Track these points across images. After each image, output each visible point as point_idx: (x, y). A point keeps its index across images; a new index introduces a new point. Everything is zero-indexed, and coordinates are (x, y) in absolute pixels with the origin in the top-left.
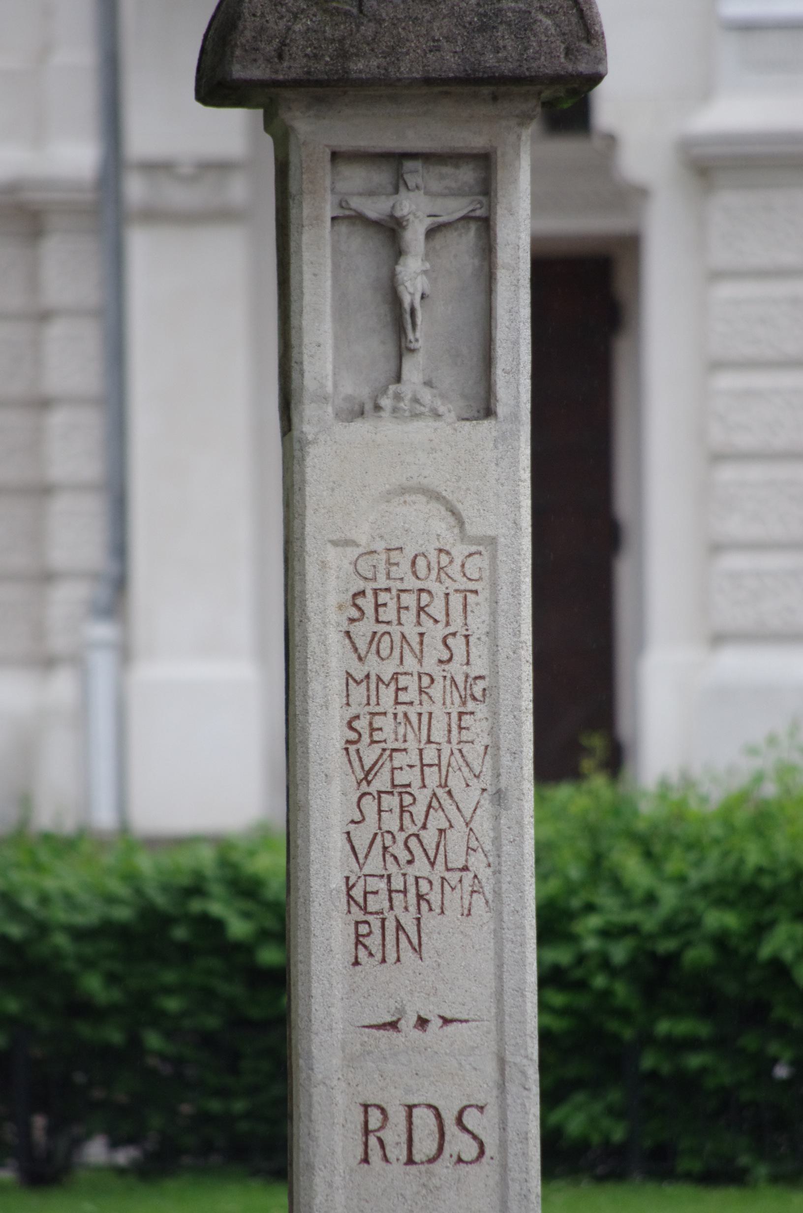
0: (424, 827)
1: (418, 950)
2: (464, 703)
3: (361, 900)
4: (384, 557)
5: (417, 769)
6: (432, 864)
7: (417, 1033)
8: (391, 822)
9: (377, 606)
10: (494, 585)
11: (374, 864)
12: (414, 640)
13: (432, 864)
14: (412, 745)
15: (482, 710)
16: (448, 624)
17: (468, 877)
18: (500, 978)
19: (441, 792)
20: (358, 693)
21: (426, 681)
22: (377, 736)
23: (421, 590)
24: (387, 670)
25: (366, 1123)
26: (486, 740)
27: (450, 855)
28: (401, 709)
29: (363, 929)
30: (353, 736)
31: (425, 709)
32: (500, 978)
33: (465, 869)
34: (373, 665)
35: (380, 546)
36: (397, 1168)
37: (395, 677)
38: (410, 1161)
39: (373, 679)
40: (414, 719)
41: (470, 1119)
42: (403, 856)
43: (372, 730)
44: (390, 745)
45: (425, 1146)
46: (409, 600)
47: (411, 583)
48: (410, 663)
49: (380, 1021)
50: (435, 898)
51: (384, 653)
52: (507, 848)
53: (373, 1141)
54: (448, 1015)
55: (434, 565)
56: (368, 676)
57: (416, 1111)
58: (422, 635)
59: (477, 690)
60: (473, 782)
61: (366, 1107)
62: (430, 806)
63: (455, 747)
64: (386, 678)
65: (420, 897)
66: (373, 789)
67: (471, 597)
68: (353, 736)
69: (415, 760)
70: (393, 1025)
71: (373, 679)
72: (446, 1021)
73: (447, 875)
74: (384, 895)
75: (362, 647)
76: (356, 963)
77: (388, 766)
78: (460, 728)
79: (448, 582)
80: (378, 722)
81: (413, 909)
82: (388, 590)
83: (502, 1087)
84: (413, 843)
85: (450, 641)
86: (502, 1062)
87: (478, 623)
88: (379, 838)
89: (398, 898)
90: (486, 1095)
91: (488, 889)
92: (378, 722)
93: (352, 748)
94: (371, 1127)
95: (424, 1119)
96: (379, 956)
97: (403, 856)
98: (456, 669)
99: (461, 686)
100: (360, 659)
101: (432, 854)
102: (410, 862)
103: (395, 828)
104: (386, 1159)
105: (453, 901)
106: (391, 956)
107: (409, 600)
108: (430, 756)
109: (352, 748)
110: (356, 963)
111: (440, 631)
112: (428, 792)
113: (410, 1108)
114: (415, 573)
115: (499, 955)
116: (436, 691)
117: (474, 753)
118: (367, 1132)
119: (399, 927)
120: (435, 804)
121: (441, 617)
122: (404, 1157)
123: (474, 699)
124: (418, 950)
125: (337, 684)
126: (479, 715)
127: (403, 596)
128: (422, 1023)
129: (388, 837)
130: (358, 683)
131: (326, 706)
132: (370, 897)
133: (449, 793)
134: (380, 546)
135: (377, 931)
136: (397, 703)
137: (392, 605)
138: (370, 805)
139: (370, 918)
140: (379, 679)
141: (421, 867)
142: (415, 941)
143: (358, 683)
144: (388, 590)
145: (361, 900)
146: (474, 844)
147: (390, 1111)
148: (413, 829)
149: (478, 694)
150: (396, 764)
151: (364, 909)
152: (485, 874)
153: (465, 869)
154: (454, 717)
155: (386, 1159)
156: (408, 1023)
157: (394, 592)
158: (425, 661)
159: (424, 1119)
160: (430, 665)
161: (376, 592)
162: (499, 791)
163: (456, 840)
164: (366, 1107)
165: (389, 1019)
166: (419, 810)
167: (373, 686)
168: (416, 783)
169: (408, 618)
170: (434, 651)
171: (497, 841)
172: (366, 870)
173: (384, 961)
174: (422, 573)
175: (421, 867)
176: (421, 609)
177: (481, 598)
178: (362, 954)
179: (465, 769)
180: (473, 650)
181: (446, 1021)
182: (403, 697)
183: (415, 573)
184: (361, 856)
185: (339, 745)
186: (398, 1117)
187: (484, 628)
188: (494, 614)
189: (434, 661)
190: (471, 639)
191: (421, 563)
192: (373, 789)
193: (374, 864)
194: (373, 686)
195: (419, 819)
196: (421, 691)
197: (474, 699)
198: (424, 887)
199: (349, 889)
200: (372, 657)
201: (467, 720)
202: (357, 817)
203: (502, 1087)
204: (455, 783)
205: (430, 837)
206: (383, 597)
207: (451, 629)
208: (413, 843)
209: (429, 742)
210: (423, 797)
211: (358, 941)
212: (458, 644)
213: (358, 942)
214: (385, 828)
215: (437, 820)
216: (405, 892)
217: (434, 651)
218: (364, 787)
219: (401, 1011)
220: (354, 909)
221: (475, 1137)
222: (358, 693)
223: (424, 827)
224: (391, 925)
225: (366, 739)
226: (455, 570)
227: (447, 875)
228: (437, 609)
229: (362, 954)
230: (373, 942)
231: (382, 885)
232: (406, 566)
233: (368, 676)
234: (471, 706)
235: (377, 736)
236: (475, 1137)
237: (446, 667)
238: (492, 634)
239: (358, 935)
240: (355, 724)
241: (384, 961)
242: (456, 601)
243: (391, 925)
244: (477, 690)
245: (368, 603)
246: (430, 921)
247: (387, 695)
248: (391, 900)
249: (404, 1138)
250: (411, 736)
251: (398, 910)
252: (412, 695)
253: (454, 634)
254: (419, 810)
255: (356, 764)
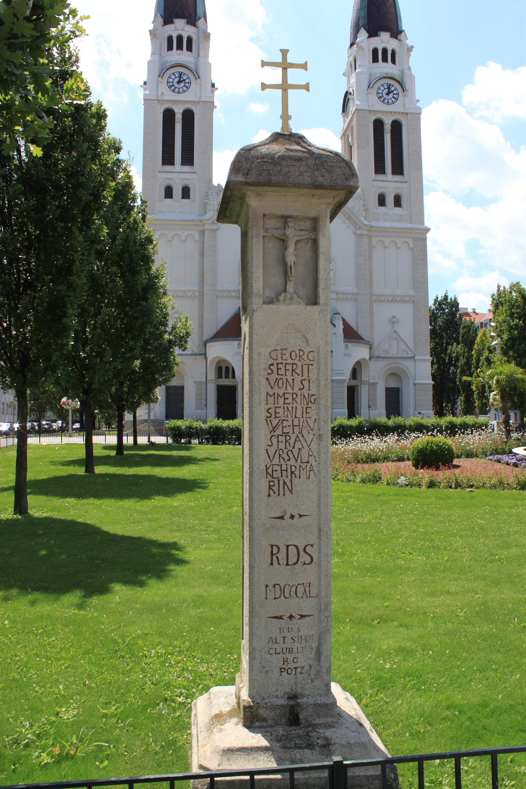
0: (294, 448)
1: (291, 491)
2: (308, 404)
3: (271, 473)
4: (280, 352)
5: (291, 427)
6: (296, 461)
7: (291, 520)
8: (282, 446)
9: (278, 369)
10: (319, 363)
11: (276, 461)
12: (291, 381)
13: (296, 461)
14: (290, 418)
15: (314, 407)
16: (302, 376)
17: (309, 465)
18: (319, 500)
19: (299, 435)
20: (271, 400)
21: (295, 396)
22: (277, 415)
23: (293, 364)
24: (281, 392)
25: (272, 551)
26: (315, 417)
27: (302, 457)
28: (286, 406)
29: (272, 484)
30: (269, 415)
31: (294, 406)
32: (319, 500)
33: (308, 462)
34: (276, 390)
35: (279, 348)
36: (283, 567)
37: (284, 394)
38: (287, 564)
39: (276, 395)
40: (290, 409)
41: (308, 549)
42: (286, 458)
43: (276, 413)
44: (282, 418)
45: (293, 559)
46: (289, 367)
47: (290, 361)
48: (289, 389)
49: (277, 516)
50: (297, 473)
51: (280, 386)
52: (322, 455)
53: (274, 557)
54: (301, 514)
55: (298, 355)
56: (274, 394)
57: (290, 547)
58: (293, 379)
59: (312, 399)
60: (311, 432)
61: (272, 546)
62: (296, 440)
63: (305, 419)
64: (281, 395)
65: (292, 472)
66: (276, 434)
67: (310, 367)
68: (269, 415)
69: (291, 424)
70: (282, 518)
71: (276, 395)
72: (301, 516)
73: (302, 465)
74: (279, 471)
75: (272, 383)
76: (269, 495)
77: (281, 426)
78: (306, 413)
79: (302, 361)
80: (278, 410)
81: (289, 476)
82: (282, 363)
83: (319, 538)
84: (290, 453)
85: (303, 382)
86: (320, 530)
87: (313, 377)
88: (278, 451)
89: (284, 473)
90: (312, 539)
91: (315, 469)
92: (278, 410)
93: (268, 419)
94: (274, 553)
95: (292, 551)
96: (277, 493)
97: (286, 458)
98: (305, 392)
99: (307, 398)
100: (271, 387)
101: (296, 457)
102: (288, 460)
103: (283, 448)
104: (279, 564)
105: (303, 474)
106: (282, 493)
107: (289, 367)
108: (296, 422)
109: (268, 419)
110: (269, 495)
111: (300, 378)
112: (295, 435)
113: (288, 546)
114: (291, 358)
115: (319, 492)
116: (298, 400)
117: (311, 422)
118: (272, 554)
119: (285, 483)
120: (298, 439)
121: (300, 373)
122: (285, 563)
123: (311, 402)
124: (291, 491)
125: (264, 396)
126: (313, 408)
127: (287, 366)
128: (292, 517)
129: (281, 451)
130: (271, 396)
131: (260, 404)
132: (274, 472)
133: (302, 436)
134: (279, 348)
135: (277, 484)
136: (284, 403)
137: (283, 368)
138: (274, 440)
139: (274, 480)
140: (278, 395)
141: (292, 462)
142: (290, 488)
143: (271, 396)
144: (282, 363)
145: (271, 473)
146: (311, 454)
147: (281, 548)
148: (290, 448)
149: (313, 402)
150: (284, 425)
151: (272, 476)
152: (314, 464)
153: (308, 462)
154: (304, 409)
155: (279, 564)
156: (287, 517)
157: (284, 364)
158: (295, 388)
159: (292, 551)
160: (296, 390)
161: (277, 364)
162: (320, 435)
163: (305, 452)
164: (272, 546)
165: (280, 515)
166: (292, 442)
167: (276, 397)
168: (291, 432)
169: (289, 373)
170: (298, 385)
171: (319, 453)
172: (273, 463)
173: (279, 495)
174: (294, 358)
175: (292, 462)
176: (293, 370)
177: (313, 367)
178: (271, 492)
179: (308, 427)
180: (311, 385)
181: (301, 516)
182: (287, 401)
183: (291, 358)
184: (271, 458)
185: (264, 418)
186: (283, 550)
187: (315, 378)
188: (318, 373)
189: (298, 389)
190: (311, 381)
191: (293, 354)
192: (276, 434)
193: (276, 461)
194: (276, 397)
195: (292, 445)
196: (293, 399)
197: (311, 402)
198: (293, 469)
199: (267, 469)
200: (276, 387)
201: (309, 410)
202: (270, 444)
203: (319, 538)
204: (304, 432)
205: (296, 451)
206: (280, 366)
207: (304, 378)
208: (290, 453)
209: (296, 417)
210: (293, 437)
211: (270, 488)
212: (306, 383)
213: (270, 488)
214: (280, 448)
215: (298, 445)
216: (287, 470)
217: (298, 385)
218: (273, 433)
219: (285, 513)
220: (269, 476)
221: (310, 555)
222: (271, 400)
223: (294, 448)
224: (281, 482)
225: (273, 416)
226: (305, 357)
227: (302, 465)
228: (299, 370)
229: (271, 492)
230: (275, 488)
231: (279, 468)
232: (288, 355)
233: (274, 394)
234: (310, 405)
235: (277, 415)
236: (310, 555)
237: (302, 391)
238: (318, 380)
239: (270, 486)
240: (270, 411)
241: (279, 495)
242: (305, 367)
243: (281, 482)
244: (312, 399)
245: (274, 368)
246: (296, 481)
247: (281, 401)
248: (282, 473)
249: (285, 556)
250: (289, 415)
251: (284, 477)
252: (290, 400)
253: (304, 380)
254: (292, 442)
255: (270, 425)
